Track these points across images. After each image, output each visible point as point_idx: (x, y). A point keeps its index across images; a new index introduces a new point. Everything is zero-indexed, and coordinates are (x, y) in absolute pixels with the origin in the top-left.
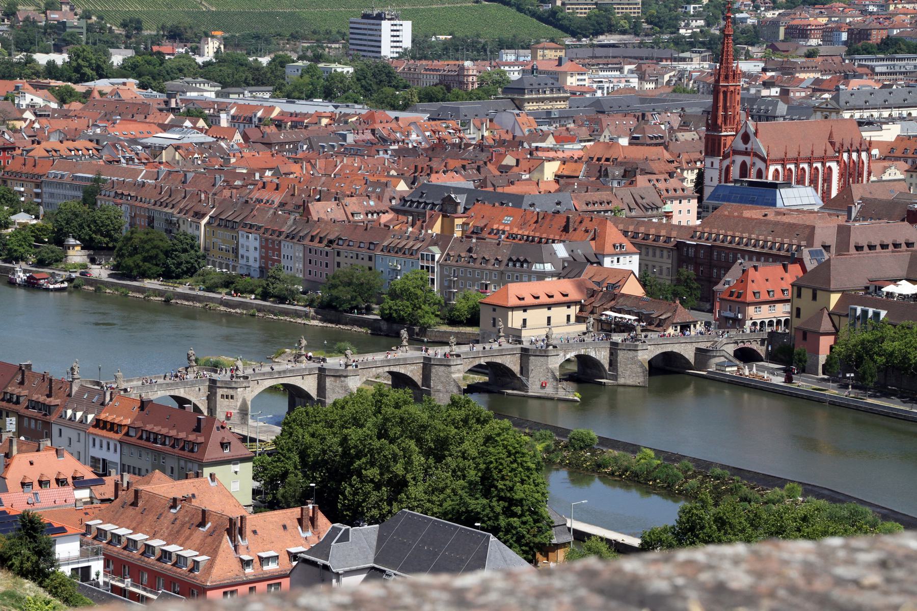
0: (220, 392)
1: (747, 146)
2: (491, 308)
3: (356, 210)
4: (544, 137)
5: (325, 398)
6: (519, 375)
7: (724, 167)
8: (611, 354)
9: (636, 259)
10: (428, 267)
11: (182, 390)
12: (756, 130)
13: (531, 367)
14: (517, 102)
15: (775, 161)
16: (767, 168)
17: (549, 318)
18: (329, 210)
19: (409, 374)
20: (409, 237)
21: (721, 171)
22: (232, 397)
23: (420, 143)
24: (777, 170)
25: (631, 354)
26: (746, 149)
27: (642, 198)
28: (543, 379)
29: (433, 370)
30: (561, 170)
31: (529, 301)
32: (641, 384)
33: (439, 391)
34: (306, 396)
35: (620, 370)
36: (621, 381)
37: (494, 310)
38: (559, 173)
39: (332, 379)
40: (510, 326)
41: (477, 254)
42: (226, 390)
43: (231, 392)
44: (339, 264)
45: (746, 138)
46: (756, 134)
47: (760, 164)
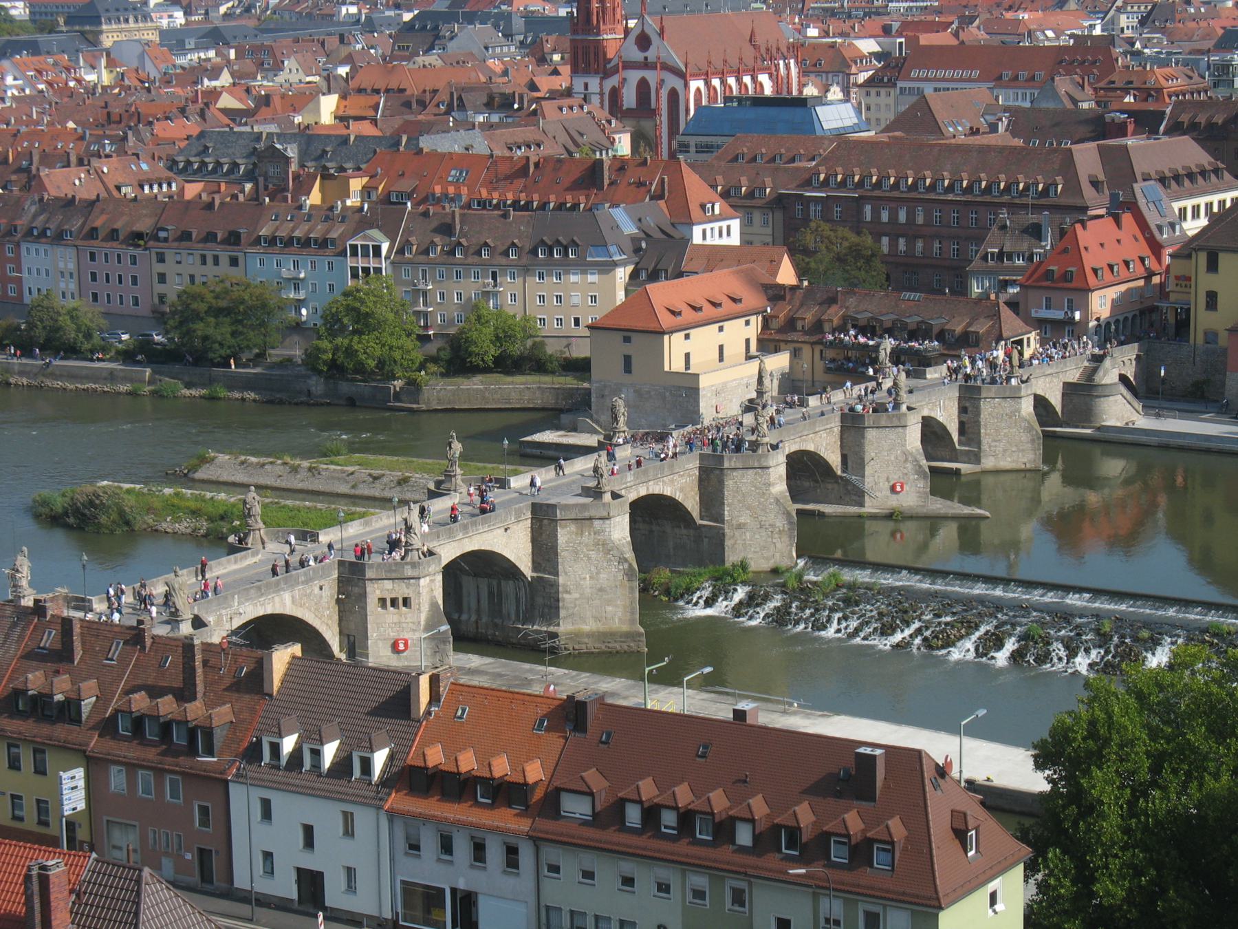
0: (375, 591)
1: (646, 54)
2: (619, 337)
3: (120, 180)
4: (215, 73)
5: (557, 574)
6: (839, 472)
7: (607, 90)
8: (963, 410)
9: (735, 224)
10: (366, 270)
11: (287, 596)
12: (662, 29)
13: (870, 451)
14: (90, 37)
15: (696, 76)
16: (686, 86)
17: (721, 348)
18: (77, 182)
19: (679, 497)
20: (310, 216)
21: (602, 94)
22: (406, 602)
23: (23, 90)
24: (698, 90)
25: (1007, 405)
26: (646, 58)
27: (582, 135)
28: (894, 478)
29: (729, 483)
30: (342, 108)
31: (689, 316)
32: (1028, 466)
33: (740, 526)
34: (508, 570)
35: (985, 441)
36: (988, 463)
37: (627, 340)
38: (341, 113)
39: (572, 527)
40: (667, 368)
41: (465, 236)
42: (388, 585)
43: (401, 590)
44: (162, 278)
45: (643, 41)
46: (661, 33)
47: (673, 82)
